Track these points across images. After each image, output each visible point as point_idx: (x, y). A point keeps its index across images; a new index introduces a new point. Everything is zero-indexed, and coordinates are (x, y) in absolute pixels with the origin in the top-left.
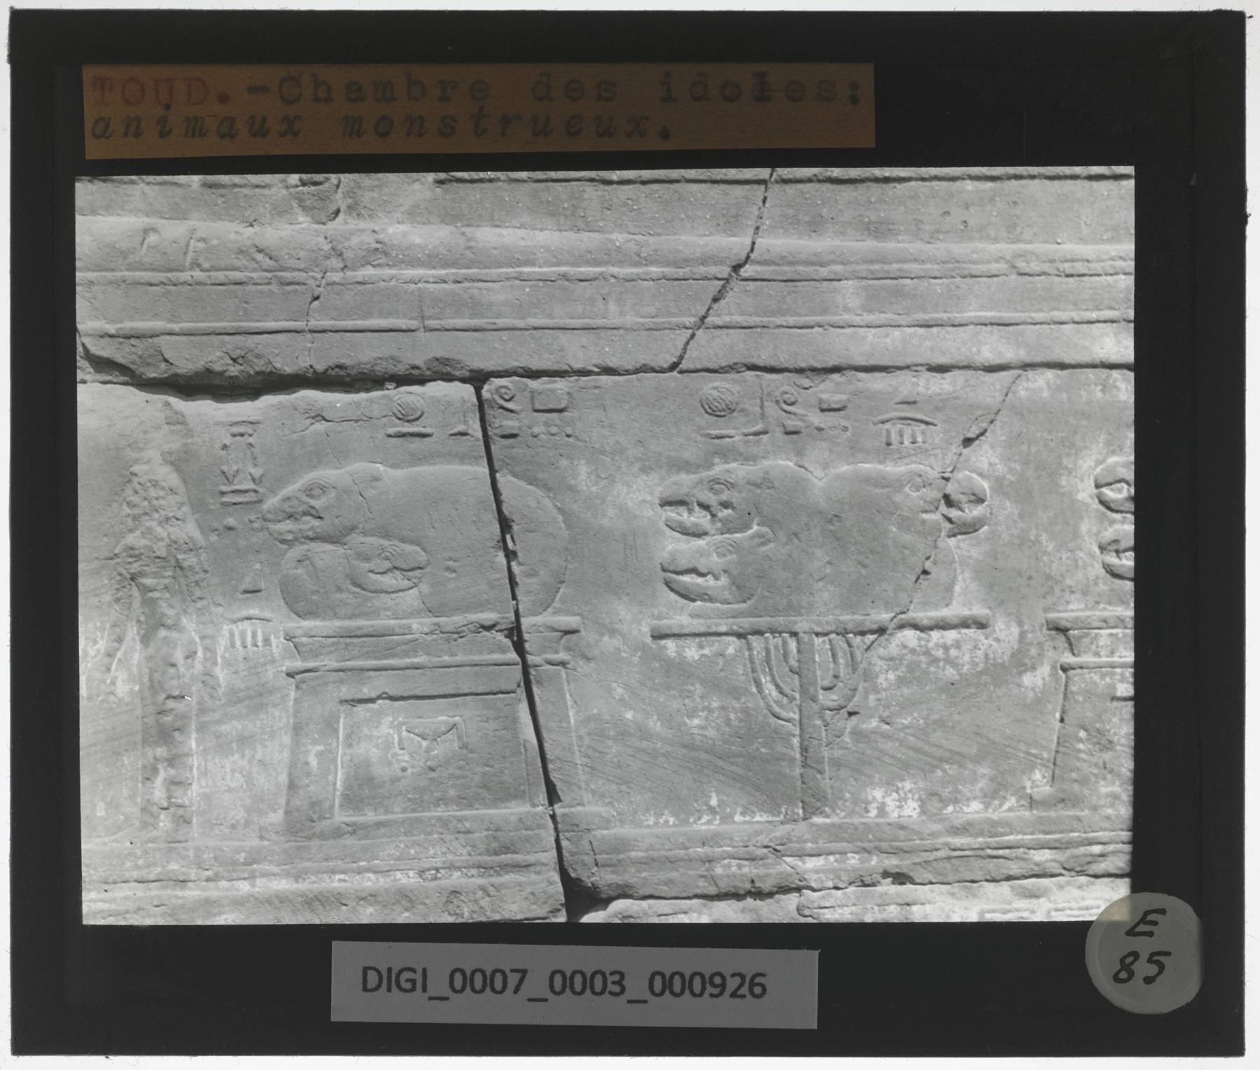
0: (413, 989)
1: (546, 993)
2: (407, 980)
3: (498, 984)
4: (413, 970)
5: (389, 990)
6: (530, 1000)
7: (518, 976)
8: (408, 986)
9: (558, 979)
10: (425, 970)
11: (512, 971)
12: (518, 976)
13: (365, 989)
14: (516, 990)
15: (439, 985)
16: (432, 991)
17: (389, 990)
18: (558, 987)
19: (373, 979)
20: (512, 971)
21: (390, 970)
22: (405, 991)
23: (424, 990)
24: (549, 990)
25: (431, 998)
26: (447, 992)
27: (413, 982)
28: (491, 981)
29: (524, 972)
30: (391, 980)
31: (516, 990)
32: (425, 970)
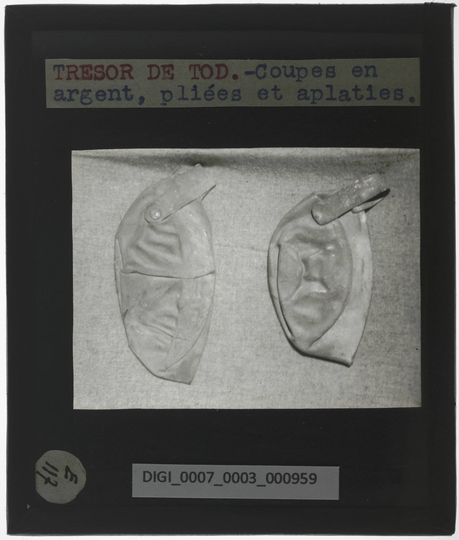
0: (165, 481)
1: (223, 482)
2: (162, 477)
3: (201, 479)
4: (165, 473)
5: (155, 481)
6: (215, 485)
7: (210, 474)
8: (162, 479)
9: (227, 476)
10: (170, 473)
11: (208, 473)
12: (210, 474)
13: (144, 481)
14: (209, 481)
15: (176, 479)
16: (173, 481)
17: (155, 481)
18: (227, 479)
19: (148, 476)
20: (208, 473)
21: (155, 472)
22: (161, 481)
23: (170, 481)
24: (223, 480)
25: (173, 485)
26: (179, 482)
27: (165, 477)
28: (199, 478)
29: (213, 473)
30: (156, 477)
31: (209, 482)
32: (170, 473)
